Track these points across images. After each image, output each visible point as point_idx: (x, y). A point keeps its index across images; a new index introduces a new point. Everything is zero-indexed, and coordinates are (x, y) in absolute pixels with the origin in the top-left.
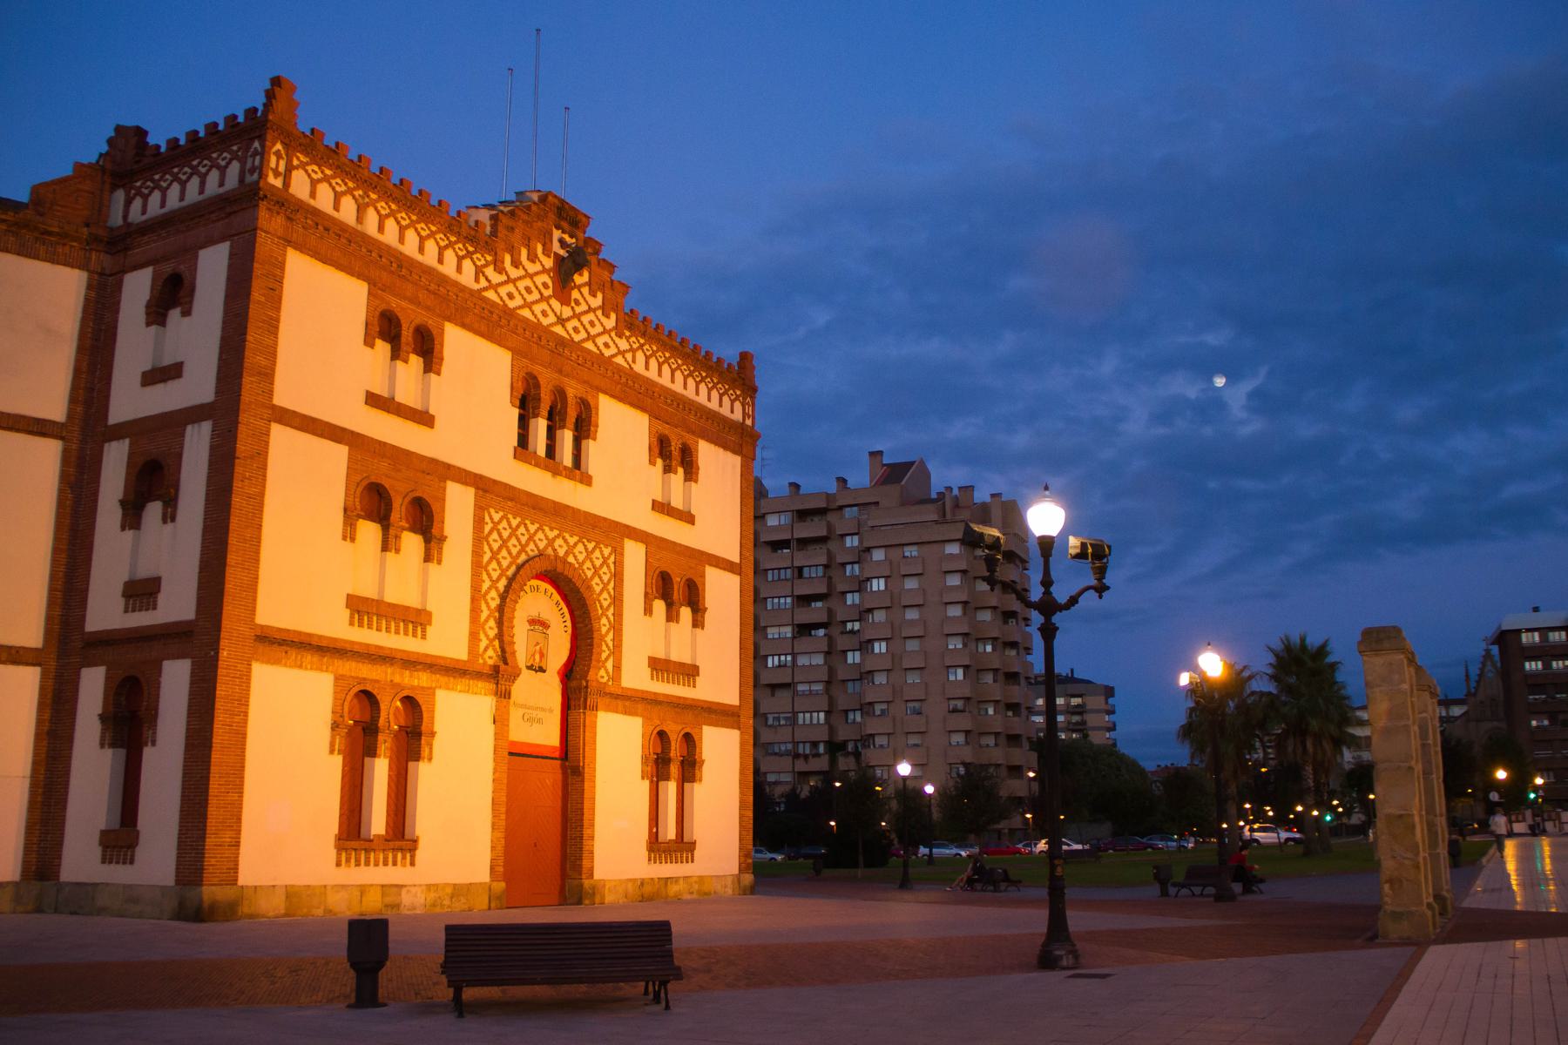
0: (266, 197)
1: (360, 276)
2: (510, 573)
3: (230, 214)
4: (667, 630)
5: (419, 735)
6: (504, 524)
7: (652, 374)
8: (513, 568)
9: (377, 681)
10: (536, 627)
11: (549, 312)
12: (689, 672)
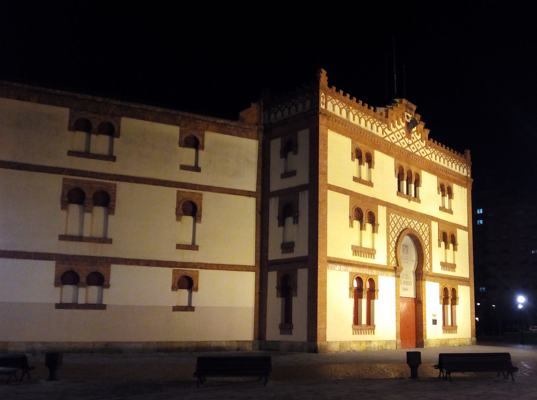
0: (321, 113)
1: (349, 137)
2: (398, 235)
4: (446, 253)
5: (374, 291)
6: (395, 218)
7: (437, 161)
8: (399, 233)
9: (362, 274)
11: (405, 143)
12: (453, 267)
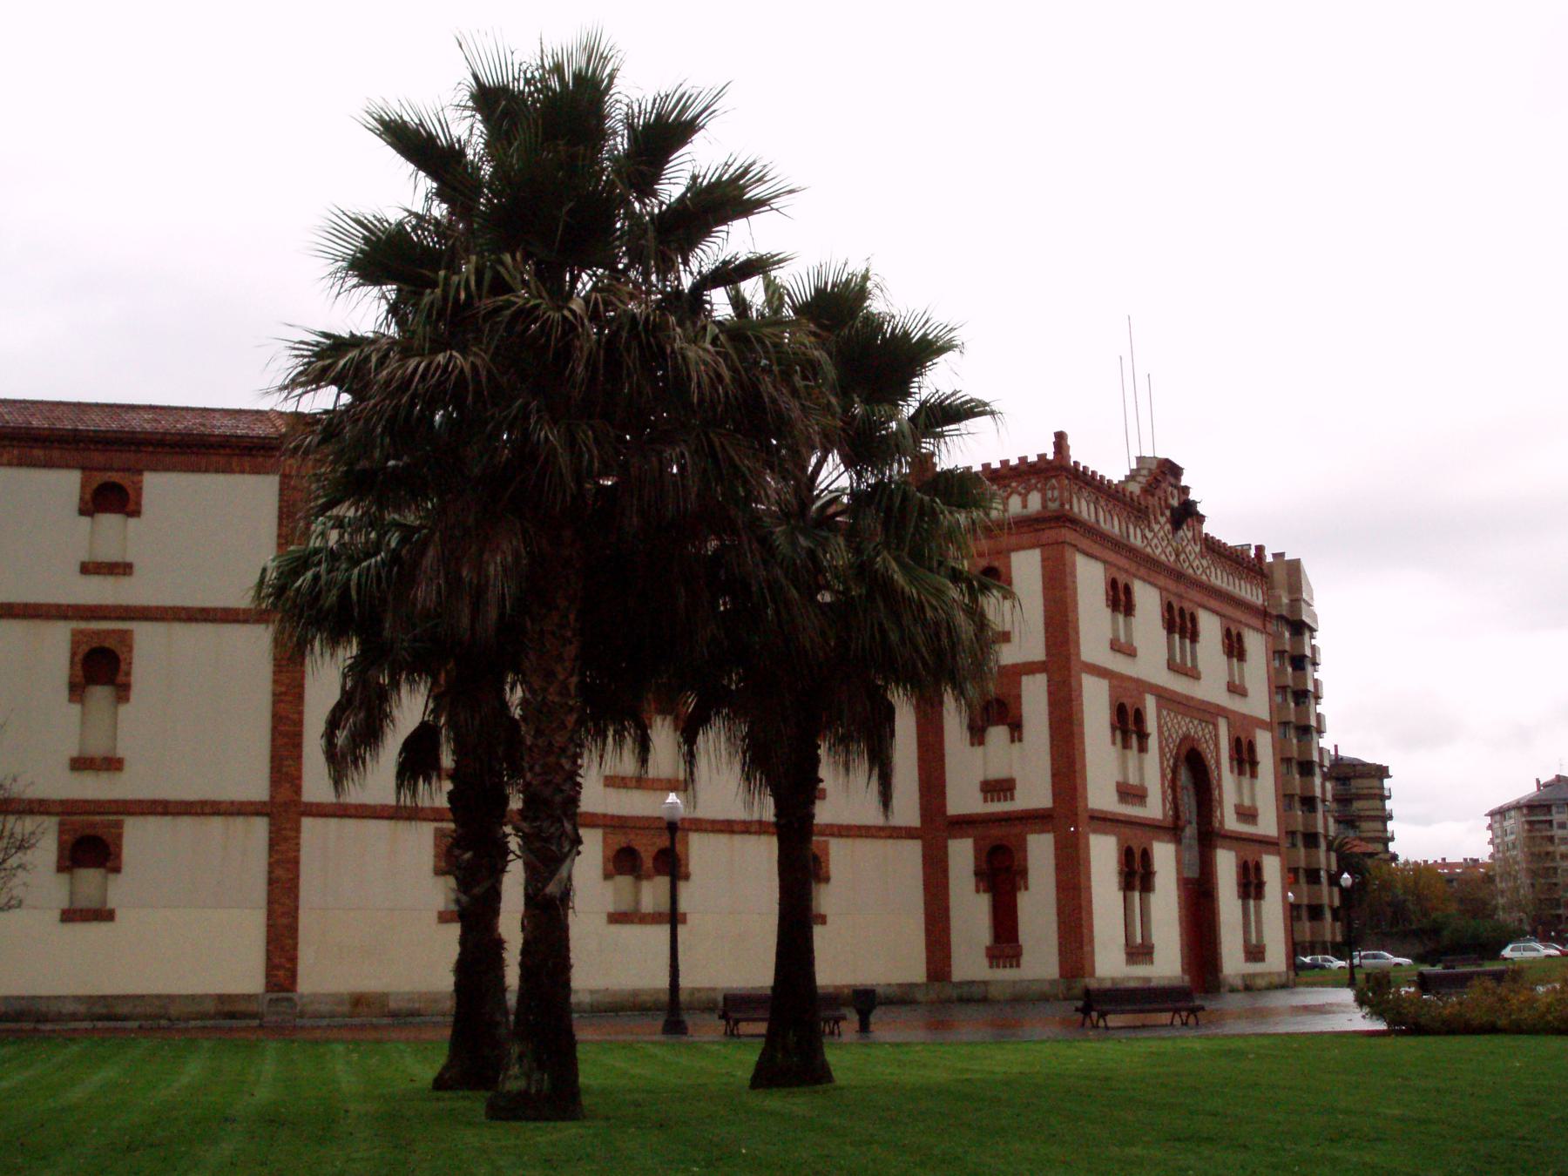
3: (1036, 530)
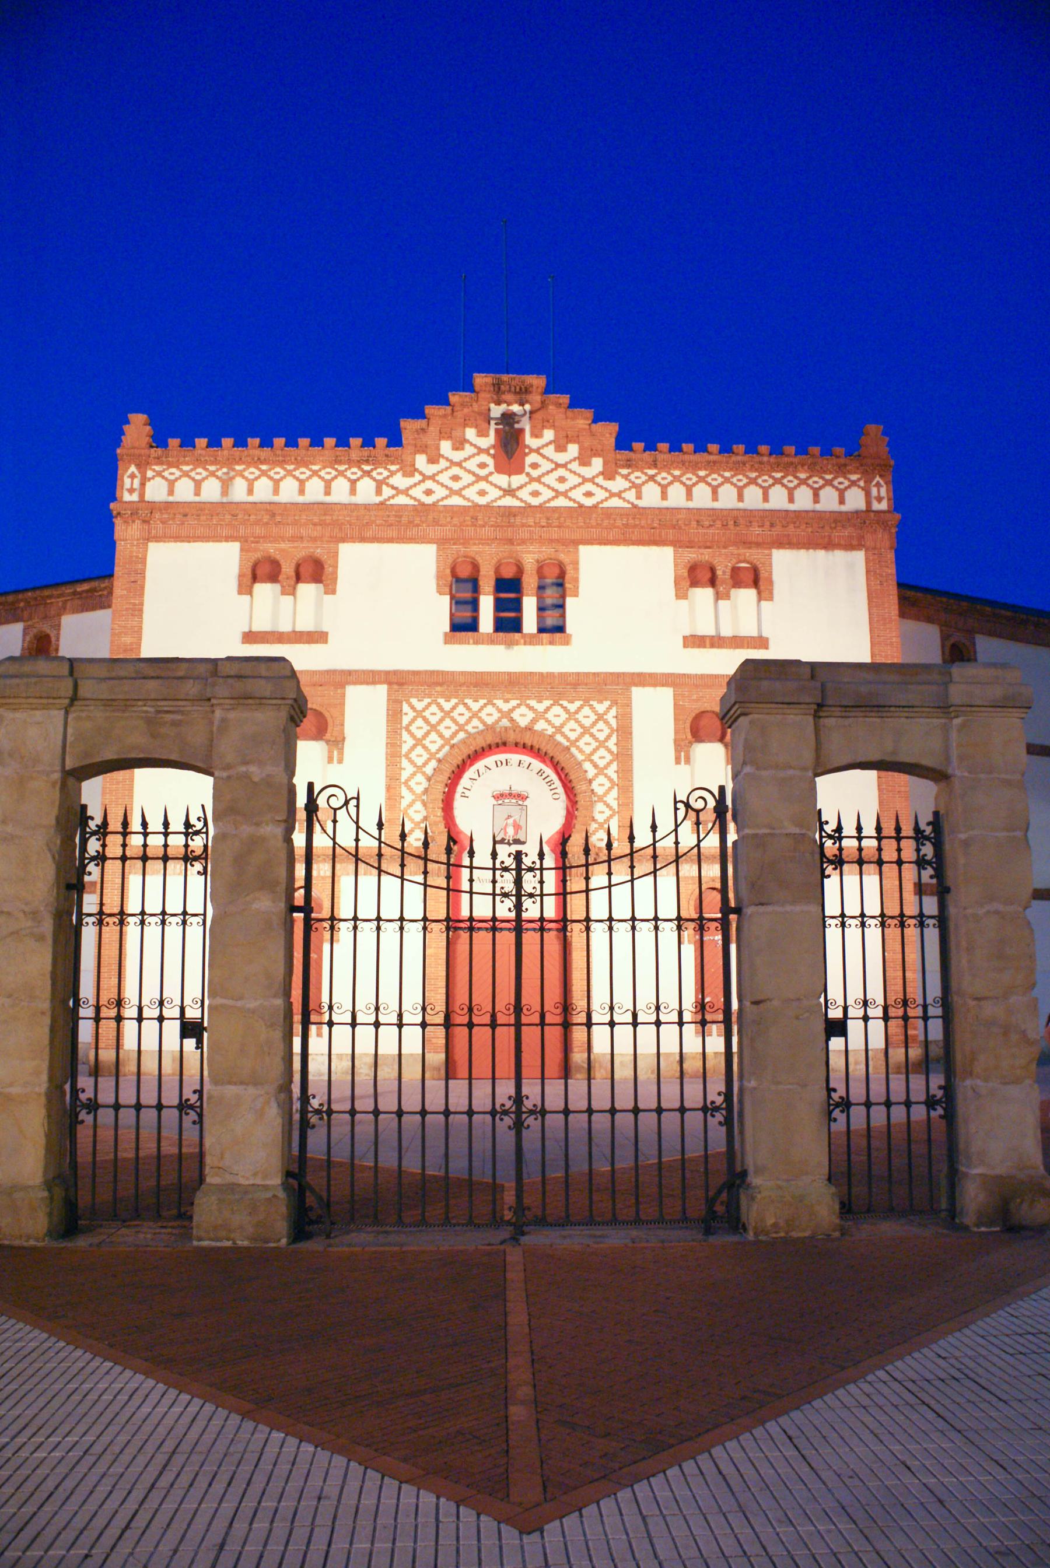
10: (507, 801)
